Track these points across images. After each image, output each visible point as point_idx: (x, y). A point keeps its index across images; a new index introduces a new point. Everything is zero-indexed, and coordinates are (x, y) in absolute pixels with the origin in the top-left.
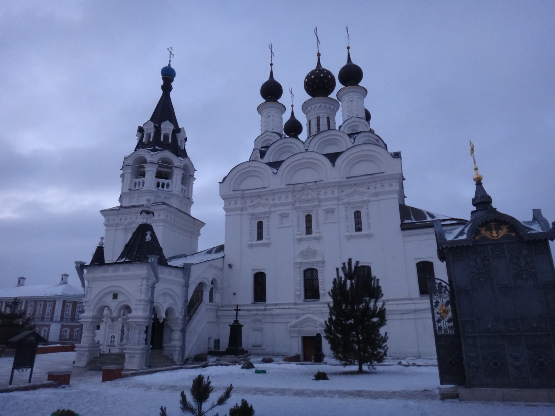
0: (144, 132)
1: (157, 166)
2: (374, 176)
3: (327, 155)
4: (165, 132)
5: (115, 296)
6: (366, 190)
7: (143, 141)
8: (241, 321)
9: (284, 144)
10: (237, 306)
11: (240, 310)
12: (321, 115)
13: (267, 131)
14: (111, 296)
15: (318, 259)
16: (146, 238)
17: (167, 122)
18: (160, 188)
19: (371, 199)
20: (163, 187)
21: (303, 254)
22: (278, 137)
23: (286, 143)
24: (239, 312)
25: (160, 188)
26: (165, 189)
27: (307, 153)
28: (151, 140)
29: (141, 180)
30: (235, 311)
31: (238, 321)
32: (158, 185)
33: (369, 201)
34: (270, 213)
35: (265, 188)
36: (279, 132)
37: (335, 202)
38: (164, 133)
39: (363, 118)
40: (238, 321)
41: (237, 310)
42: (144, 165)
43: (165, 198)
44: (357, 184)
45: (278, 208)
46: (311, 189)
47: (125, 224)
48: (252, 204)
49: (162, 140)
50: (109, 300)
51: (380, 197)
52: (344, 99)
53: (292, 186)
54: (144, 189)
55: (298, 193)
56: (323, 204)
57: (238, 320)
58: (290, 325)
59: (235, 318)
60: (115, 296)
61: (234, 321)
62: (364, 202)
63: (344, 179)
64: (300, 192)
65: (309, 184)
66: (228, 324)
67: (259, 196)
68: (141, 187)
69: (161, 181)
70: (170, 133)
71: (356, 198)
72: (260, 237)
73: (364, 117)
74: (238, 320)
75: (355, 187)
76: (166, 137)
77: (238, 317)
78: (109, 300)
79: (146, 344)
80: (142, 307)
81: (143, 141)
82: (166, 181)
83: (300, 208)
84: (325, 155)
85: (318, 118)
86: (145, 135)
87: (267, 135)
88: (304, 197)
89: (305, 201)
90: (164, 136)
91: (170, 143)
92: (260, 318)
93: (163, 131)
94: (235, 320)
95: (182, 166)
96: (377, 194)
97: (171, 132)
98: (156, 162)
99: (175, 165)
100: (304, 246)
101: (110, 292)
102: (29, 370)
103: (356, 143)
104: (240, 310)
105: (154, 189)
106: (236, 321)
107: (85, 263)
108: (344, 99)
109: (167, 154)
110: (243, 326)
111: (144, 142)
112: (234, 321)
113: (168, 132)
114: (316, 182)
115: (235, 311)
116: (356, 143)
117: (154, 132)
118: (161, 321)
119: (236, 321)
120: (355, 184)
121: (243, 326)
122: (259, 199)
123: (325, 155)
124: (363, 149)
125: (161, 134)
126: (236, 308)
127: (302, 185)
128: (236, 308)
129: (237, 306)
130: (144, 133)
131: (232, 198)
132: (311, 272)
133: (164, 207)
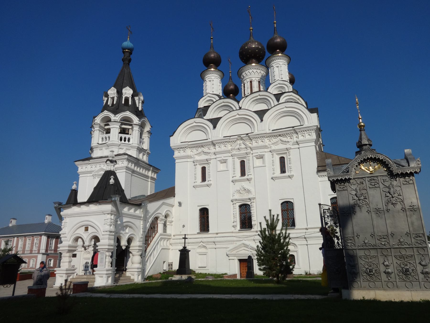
0: (109, 96)
1: (120, 123)
2: (295, 128)
3: (256, 112)
4: (125, 96)
5: (87, 229)
6: (288, 139)
7: (108, 104)
8: (188, 248)
9: (221, 103)
10: (185, 235)
11: (187, 238)
12: (254, 79)
13: (209, 93)
14: (83, 228)
15: (250, 196)
16: (110, 182)
17: (128, 88)
18: (123, 141)
19: (292, 147)
20: (125, 141)
21: (239, 192)
22: (218, 98)
23: (224, 102)
24: (186, 239)
25: (123, 141)
26: (127, 142)
27: (241, 110)
28: (115, 103)
29: (107, 135)
30: (184, 239)
31: (186, 247)
32: (121, 140)
34: (211, 159)
35: (207, 139)
36: (219, 94)
38: (125, 97)
39: (287, 81)
40: (186, 247)
41: (185, 238)
42: (109, 123)
43: (127, 149)
44: (281, 135)
45: (218, 156)
46: (244, 140)
47: (95, 171)
48: (197, 152)
49: (123, 103)
50: (81, 232)
51: (301, 145)
52: (271, 66)
53: (229, 137)
54: (109, 142)
57: (186, 246)
58: (228, 249)
59: (184, 245)
60: (87, 229)
61: (183, 247)
63: (271, 132)
64: (235, 142)
65: (242, 136)
66: (178, 250)
67: (202, 146)
68: (107, 141)
69: (123, 136)
70: (129, 97)
71: (281, 146)
72: (204, 179)
73: (288, 80)
74: (186, 246)
75: (280, 137)
76: (127, 99)
77: (186, 245)
78: (81, 232)
79: (111, 267)
80: (108, 236)
81: (108, 104)
82: (127, 136)
84: (255, 112)
85: (251, 82)
86: (110, 99)
87: (209, 97)
90: (125, 99)
91: (130, 105)
92: (204, 245)
93: (124, 95)
94: (184, 246)
95: (140, 123)
97: (131, 96)
98: (119, 121)
99: (135, 123)
100: (238, 185)
101: (83, 226)
102: (12, 286)
103: (280, 103)
104: (187, 238)
105: (117, 143)
106: (185, 247)
107: (62, 203)
108: (271, 66)
109: (128, 114)
110: (190, 251)
111: (109, 105)
112: (183, 247)
113: (128, 96)
114: (247, 134)
115: (184, 239)
116: (280, 102)
117: (116, 96)
118: (124, 248)
119: (185, 247)
120: (280, 135)
121: (190, 251)
122: (203, 148)
123: (255, 112)
124: (287, 106)
125: (123, 97)
126: (184, 237)
127: (236, 137)
128: (184, 237)
129: (185, 235)
130: (109, 97)
131: (181, 148)
132: (245, 207)
133: (126, 156)
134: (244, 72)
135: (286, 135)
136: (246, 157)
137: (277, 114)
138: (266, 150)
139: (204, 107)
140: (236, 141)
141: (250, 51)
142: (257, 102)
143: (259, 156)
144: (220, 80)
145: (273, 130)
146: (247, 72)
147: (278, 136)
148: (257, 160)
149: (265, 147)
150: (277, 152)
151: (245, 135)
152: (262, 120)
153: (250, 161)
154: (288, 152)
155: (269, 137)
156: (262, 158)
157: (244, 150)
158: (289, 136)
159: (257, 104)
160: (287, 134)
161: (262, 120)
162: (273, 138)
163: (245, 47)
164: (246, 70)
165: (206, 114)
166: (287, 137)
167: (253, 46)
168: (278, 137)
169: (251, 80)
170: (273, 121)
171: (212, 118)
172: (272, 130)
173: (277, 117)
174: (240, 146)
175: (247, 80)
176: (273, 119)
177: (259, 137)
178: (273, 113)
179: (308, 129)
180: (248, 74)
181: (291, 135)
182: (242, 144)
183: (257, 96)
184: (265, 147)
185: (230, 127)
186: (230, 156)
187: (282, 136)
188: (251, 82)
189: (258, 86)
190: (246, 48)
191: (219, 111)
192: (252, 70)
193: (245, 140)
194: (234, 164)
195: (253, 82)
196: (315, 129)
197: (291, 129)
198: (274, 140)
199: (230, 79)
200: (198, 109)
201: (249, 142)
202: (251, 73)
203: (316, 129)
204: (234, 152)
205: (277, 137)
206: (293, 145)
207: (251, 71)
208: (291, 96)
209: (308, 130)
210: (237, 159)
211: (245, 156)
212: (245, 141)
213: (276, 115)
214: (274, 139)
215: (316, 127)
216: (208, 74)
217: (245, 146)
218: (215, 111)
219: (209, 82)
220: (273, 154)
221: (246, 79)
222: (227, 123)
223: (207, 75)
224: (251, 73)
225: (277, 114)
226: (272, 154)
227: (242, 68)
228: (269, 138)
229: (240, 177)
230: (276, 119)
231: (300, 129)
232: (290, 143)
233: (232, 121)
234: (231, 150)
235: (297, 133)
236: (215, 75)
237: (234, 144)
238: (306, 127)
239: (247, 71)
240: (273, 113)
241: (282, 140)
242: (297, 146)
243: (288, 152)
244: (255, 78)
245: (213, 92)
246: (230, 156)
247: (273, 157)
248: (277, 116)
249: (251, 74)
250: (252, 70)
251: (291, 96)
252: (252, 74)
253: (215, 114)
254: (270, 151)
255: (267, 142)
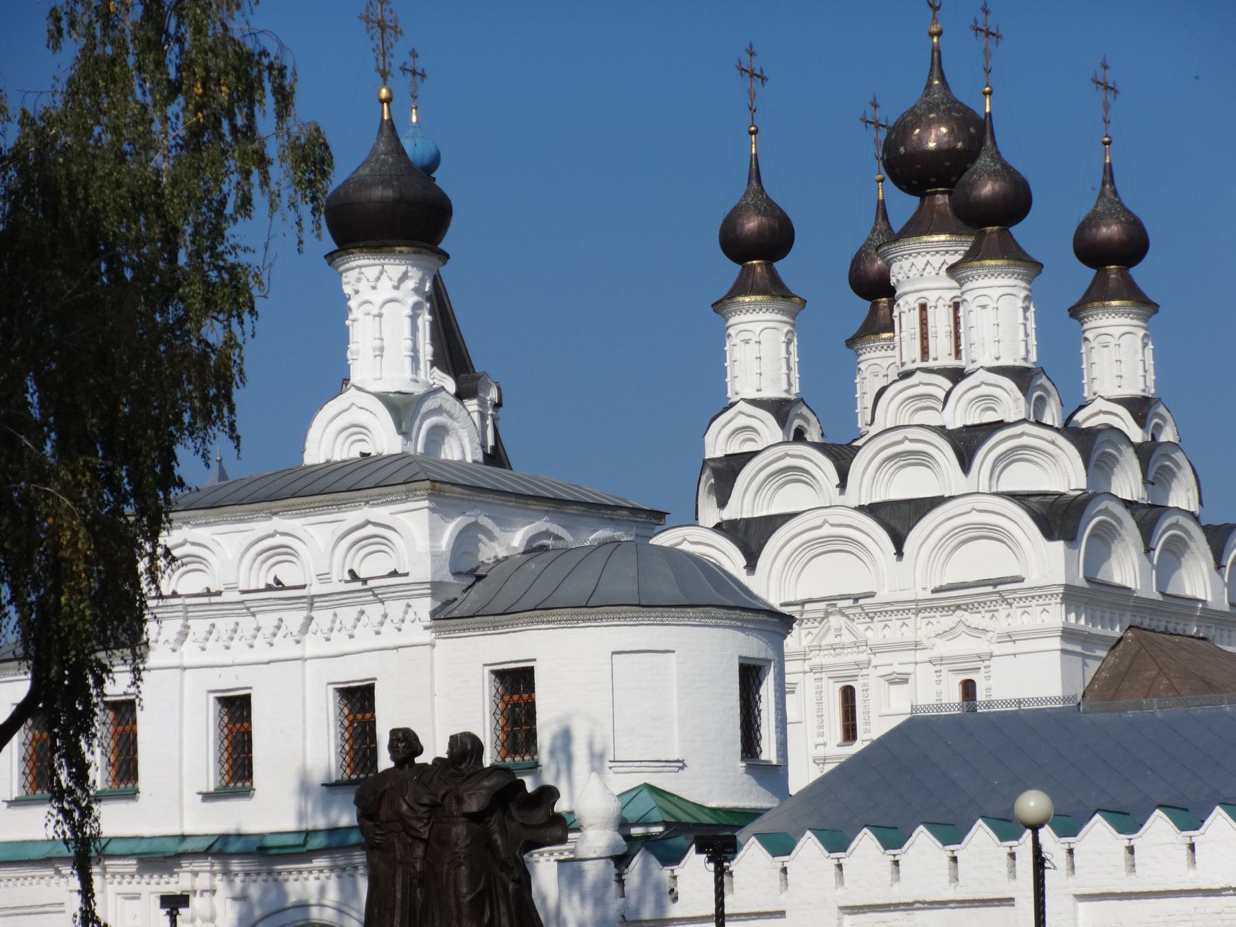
12: (931, 298)
33: (992, 656)
37: (909, 656)
46: (847, 616)
51: (1021, 646)
55: (816, 624)
56: (876, 660)
62: (980, 658)
63: (930, 595)
64: (820, 623)
65: (841, 604)
71: (965, 645)
75: (959, 612)
83: (821, 669)
85: (923, 307)
87: (741, 413)
88: (830, 639)
89: (835, 649)
96: (1010, 637)
120: (958, 607)
127: (822, 605)
134: (895, 262)
135: (977, 608)
136: (857, 676)
137: (947, 534)
138: (920, 656)
139: (727, 456)
140: (823, 619)
141: (918, 166)
142: (903, 460)
143: (895, 676)
144: (787, 328)
145: (935, 591)
146: (906, 264)
147: (952, 608)
148: (892, 687)
149: (916, 646)
150: (950, 666)
151: (850, 602)
152: (899, 553)
153: (869, 692)
154: (985, 667)
155: (926, 610)
156: (906, 681)
157: (849, 650)
158: (986, 611)
159: (902, 467)
160: (979, 603)
161: (899, 553)
162: (938, 614)
163: (898, 149)
164: (902, 256)
165: (730, 501)
166: (980, 612)
167: (932, 145)
168: (954, 611)
169: (923, 301)
170: (935, 557)
171: (750, 516)
172: (933, 588)
173: (949, 541)
174: (836, 636)
175: (907, 298)
176: (934, 549)
177: (892, 611)
178: (937, 527)
179: (1038, 593)
180: (911, 275)
181: (992, 608)
182: (844, 631)
183: (900, 442)
184: (916, 646)
185: (806, 564)
186: (807, 669)
187: (966, 610)
188: (923, 307)
189: (894, 414)
190: (902, 150)
191: (774, 487)
192: (924, 260)
193: (852, 616)
194: (820, 702)
195: (930, 312)
196: (1060, 595)
197: (990, 589)
198: (945, 621)
199: (877, 218)
200: (705, 462)
201: (866, 625)
202: (924, 269)
203: (1063, 593)
204: (817, 659)
205: (950, 612)
206: (998, 642)
207: (920, 261)
208: (1022, 434)
209: (1040, 596)
210: (831, 681)
211: (854, 672)
212: (853, 620)
213: (944, 537)
214: (942, 616)
215: (1061, 590)
216: (738, 313)
217: (854, 639)
218: (759, 489)
219: (742, 344)
220: (940, 671)
221: (905, 294)
222: (793, 554)
223: (733, 314)
224: (924, 269)
225: (947, 534)
226: (936, 672)
227: (886, 248)
228: (927, 614)
229: (839, 746)
230: (948, 550)
231: (1014, 591)
232: (990, 634)
233: (792, 563)
234: (807, 649)
235: (1011, 605)
236: (768, 316)
237: (818, 627)
238: (1032, 588)
239: (907, 259)
240: (937, 527)
241: (967, 623)
242: (1009, 648)
243: (985, 667)
244: (936, 294)
245: (759, 390)
246: (805, 673)
247: (939, 682)
248: (947, 540)
249: (922, 275)
250: (924, 260)
251: (1022, 434)
252: (925, 274)
253: (762, 498)
254: (930, 662)
255: (922, 628)
